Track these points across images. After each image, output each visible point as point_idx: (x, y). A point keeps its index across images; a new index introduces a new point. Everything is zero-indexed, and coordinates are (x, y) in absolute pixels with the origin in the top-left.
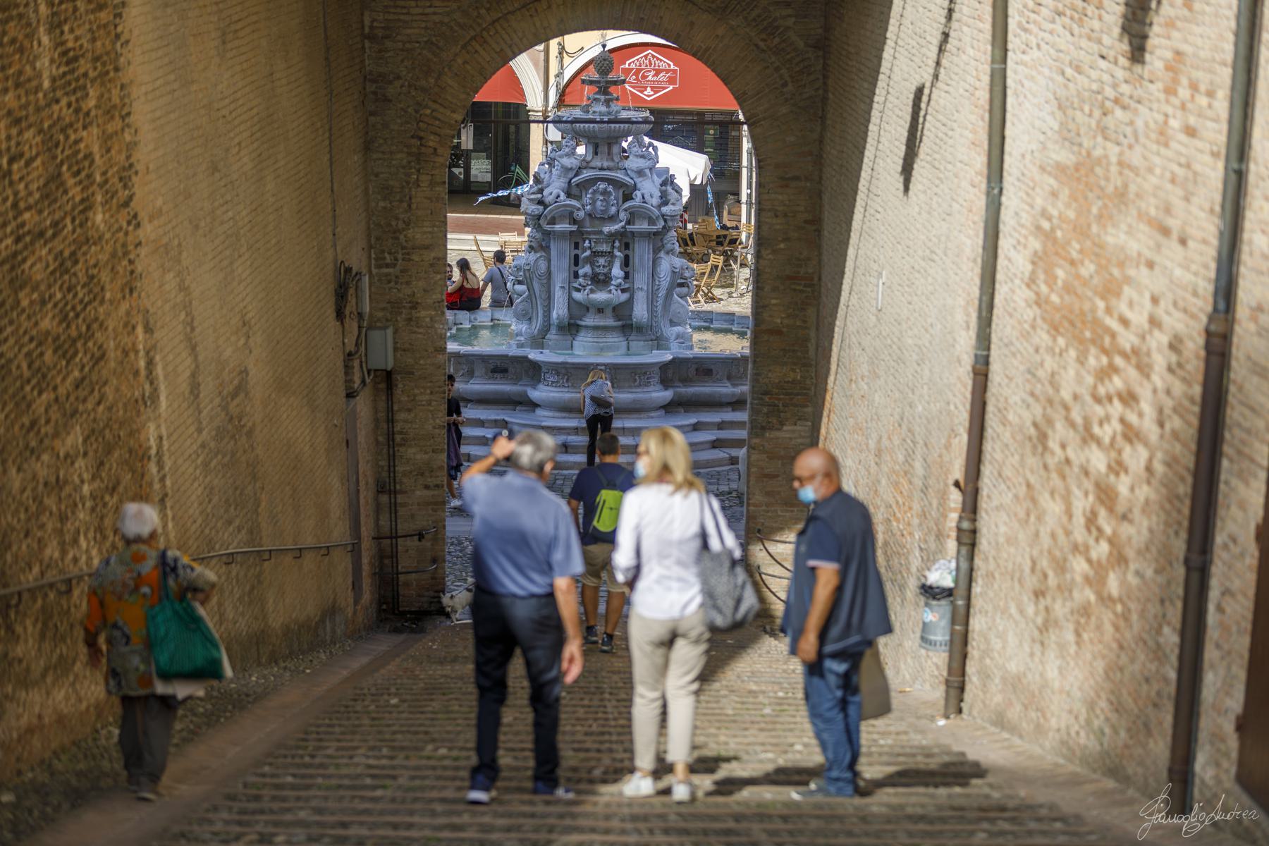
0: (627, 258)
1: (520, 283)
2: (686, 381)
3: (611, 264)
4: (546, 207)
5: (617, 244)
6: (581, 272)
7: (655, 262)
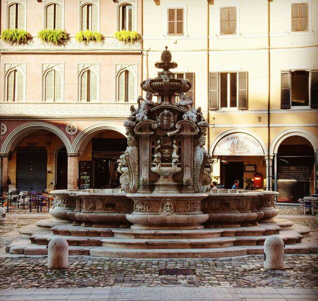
1: (124, 166)
2: (216, 210)
3: (171, 152)
4: (137, 123)
5: (175, 142)
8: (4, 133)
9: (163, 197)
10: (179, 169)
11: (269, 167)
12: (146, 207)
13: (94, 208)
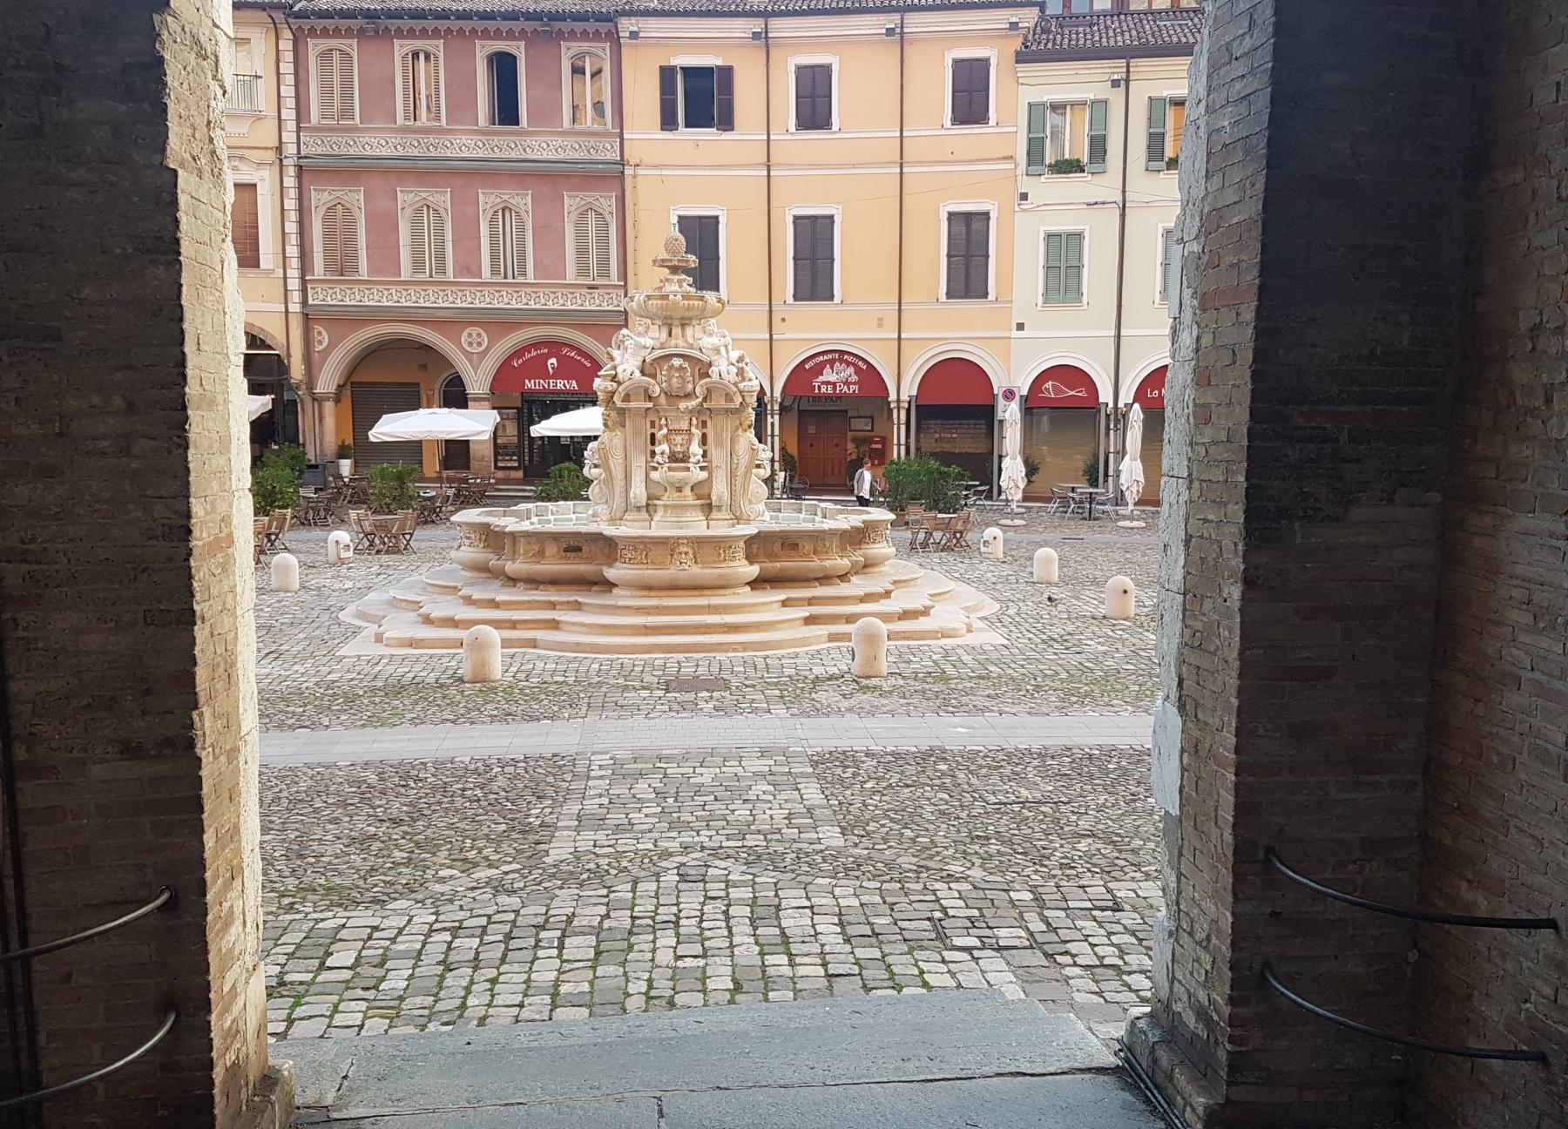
0: (704, 436)
1: (596, 466)
2: (772, 556)
3: (690, 441)
4: (619, 383)
5: (694, 421)
6: (658, 449)
7: (733, 440)
8: (321, 348)
9: (673, 537)
10: (704, 475)
11: (899, 424)
12: (641, 554)
13: (541, 554)
